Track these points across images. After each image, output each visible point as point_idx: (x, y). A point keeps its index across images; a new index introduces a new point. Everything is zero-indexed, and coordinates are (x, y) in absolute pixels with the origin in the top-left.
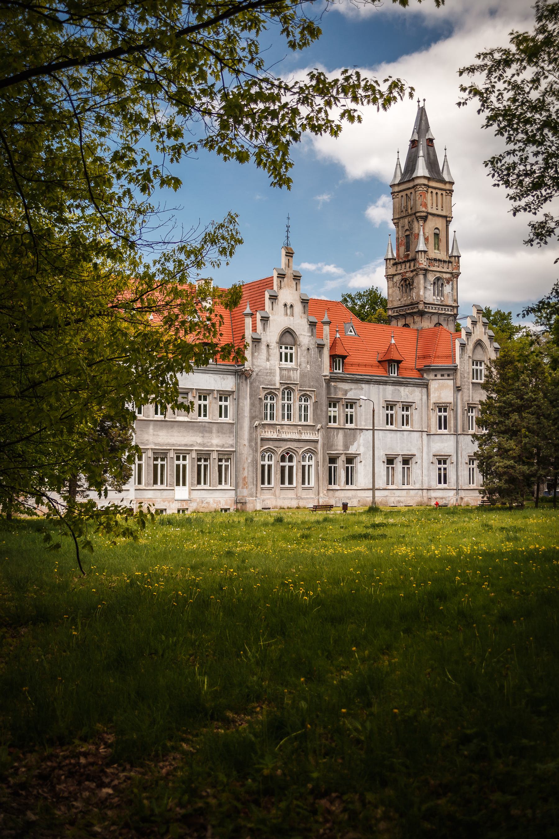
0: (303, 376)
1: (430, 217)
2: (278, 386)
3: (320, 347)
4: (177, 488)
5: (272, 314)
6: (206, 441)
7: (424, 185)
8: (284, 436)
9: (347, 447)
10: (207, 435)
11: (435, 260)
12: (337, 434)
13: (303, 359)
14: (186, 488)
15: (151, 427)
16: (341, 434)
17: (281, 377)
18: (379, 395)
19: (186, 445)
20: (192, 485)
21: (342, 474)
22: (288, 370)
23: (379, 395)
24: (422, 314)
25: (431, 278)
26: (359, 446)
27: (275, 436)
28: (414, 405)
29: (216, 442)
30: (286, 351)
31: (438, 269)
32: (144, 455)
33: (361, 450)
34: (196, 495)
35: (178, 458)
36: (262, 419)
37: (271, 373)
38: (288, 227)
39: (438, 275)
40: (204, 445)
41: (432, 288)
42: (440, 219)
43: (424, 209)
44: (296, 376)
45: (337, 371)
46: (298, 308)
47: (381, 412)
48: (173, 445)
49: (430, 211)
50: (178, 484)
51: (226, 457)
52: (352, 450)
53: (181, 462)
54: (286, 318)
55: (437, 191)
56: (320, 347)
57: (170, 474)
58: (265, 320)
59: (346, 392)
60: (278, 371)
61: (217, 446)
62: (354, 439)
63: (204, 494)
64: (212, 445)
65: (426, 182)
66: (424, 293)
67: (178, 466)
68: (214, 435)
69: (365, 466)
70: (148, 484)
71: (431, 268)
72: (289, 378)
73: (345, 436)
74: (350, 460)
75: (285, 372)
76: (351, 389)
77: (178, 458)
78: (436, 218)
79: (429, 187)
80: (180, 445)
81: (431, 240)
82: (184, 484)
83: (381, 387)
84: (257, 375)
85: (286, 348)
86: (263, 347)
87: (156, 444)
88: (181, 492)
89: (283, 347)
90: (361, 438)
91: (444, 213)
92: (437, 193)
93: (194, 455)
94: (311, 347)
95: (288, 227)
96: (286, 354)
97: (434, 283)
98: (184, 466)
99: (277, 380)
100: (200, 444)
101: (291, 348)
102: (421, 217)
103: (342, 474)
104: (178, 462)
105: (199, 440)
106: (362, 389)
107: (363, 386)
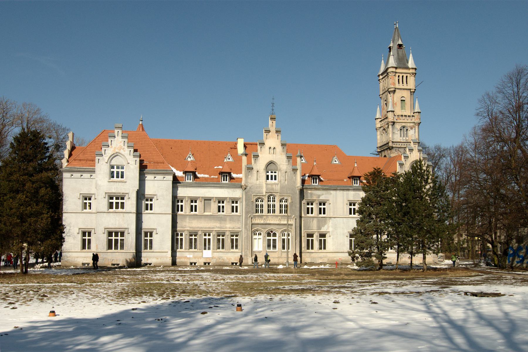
0: (282, 188)
1: (397, 91)
2: (264, 194)
3: (295, 170)
4: (204, 251)
5: (261, 154)
6: (222, 225)
7: (392, 72)
8: (268, 222)
9: (319, 228)
10: (223, 222)
11: (402, 116)
12: (313, 221)
13: (282, 178)
14: (210, 251)
15: (188, 218)
16: (315, 221)
17: (267, 189)
18: (343, 197)
19: (209, 228)
20: (213, 249)
21: (316, 244)
22: (272, 184)
23: (343, 197)
24: (391, 148)
25: (398, 126)
26: (328, 227)
27: (262, 222)
28: (127, 195)
29: (229, 226)
30: (272, 174)
31: (404, 121)
32: (211, 234)
33: (330, 229)
34: (216, 255)
35: (205, 235)
36: (253, 213)
37: (260, 186)
38: (273, 104)
39: (403, 124)
40: (221, 228)
41: (399, 132)
42: (406, 91)
43: (393, 86)
44: (278, 188)
45: (225, 182)
46: (279, 148)
47: (345, 207)
48: (201, 228)
49: (397, 87)
50: (205, 249)
51: (236, 234)
52: (323, 230)
53: (207, 237)
54: (270, 155)
55: (403, 74)
56: (295, 170)
57: (200, 243)
58: (256, 156)
59: (319, 196)
60: (264, 185)
61: (230, 228)
62: (325, 223)
63: (221, 255)
64: (226, 228)
65: (394, 70)
66: (393, 136)
67: (205, 239)
68: (228, 222)
69: (333, 239)
70: (185, 249)
71: (398, 121)
72: (273, 189)
73: (318, 222)
74: (323, 235)
75: (269, 186)
76: (323, 194)
77: (205, 235)
78: (402, 91)
79: (396, 73)
80: (205, 228)
81: (399, 103)
82: (209, 249)
83: (345, 192)
84: (250, 188)
85: (272, 172)
86: (254, 172)
87: (190, 228)
88: (207, 254)
89: (270, 172)
90: (330, 223)
91: (409, 88)
92: (403, 76)
93: (186, 232)
94: (288, 171)
95: (273, 104)
96: (272, 176)
97: (401, 130)
98: (209, 240)
99: (264, 190)
100: (218, 227)
101: (275, 172)
102: (391, 91)
103: (316, 244)
104: (205, 237)
105: (218, 225)
106: (331, 194)
107: (332, 192)
